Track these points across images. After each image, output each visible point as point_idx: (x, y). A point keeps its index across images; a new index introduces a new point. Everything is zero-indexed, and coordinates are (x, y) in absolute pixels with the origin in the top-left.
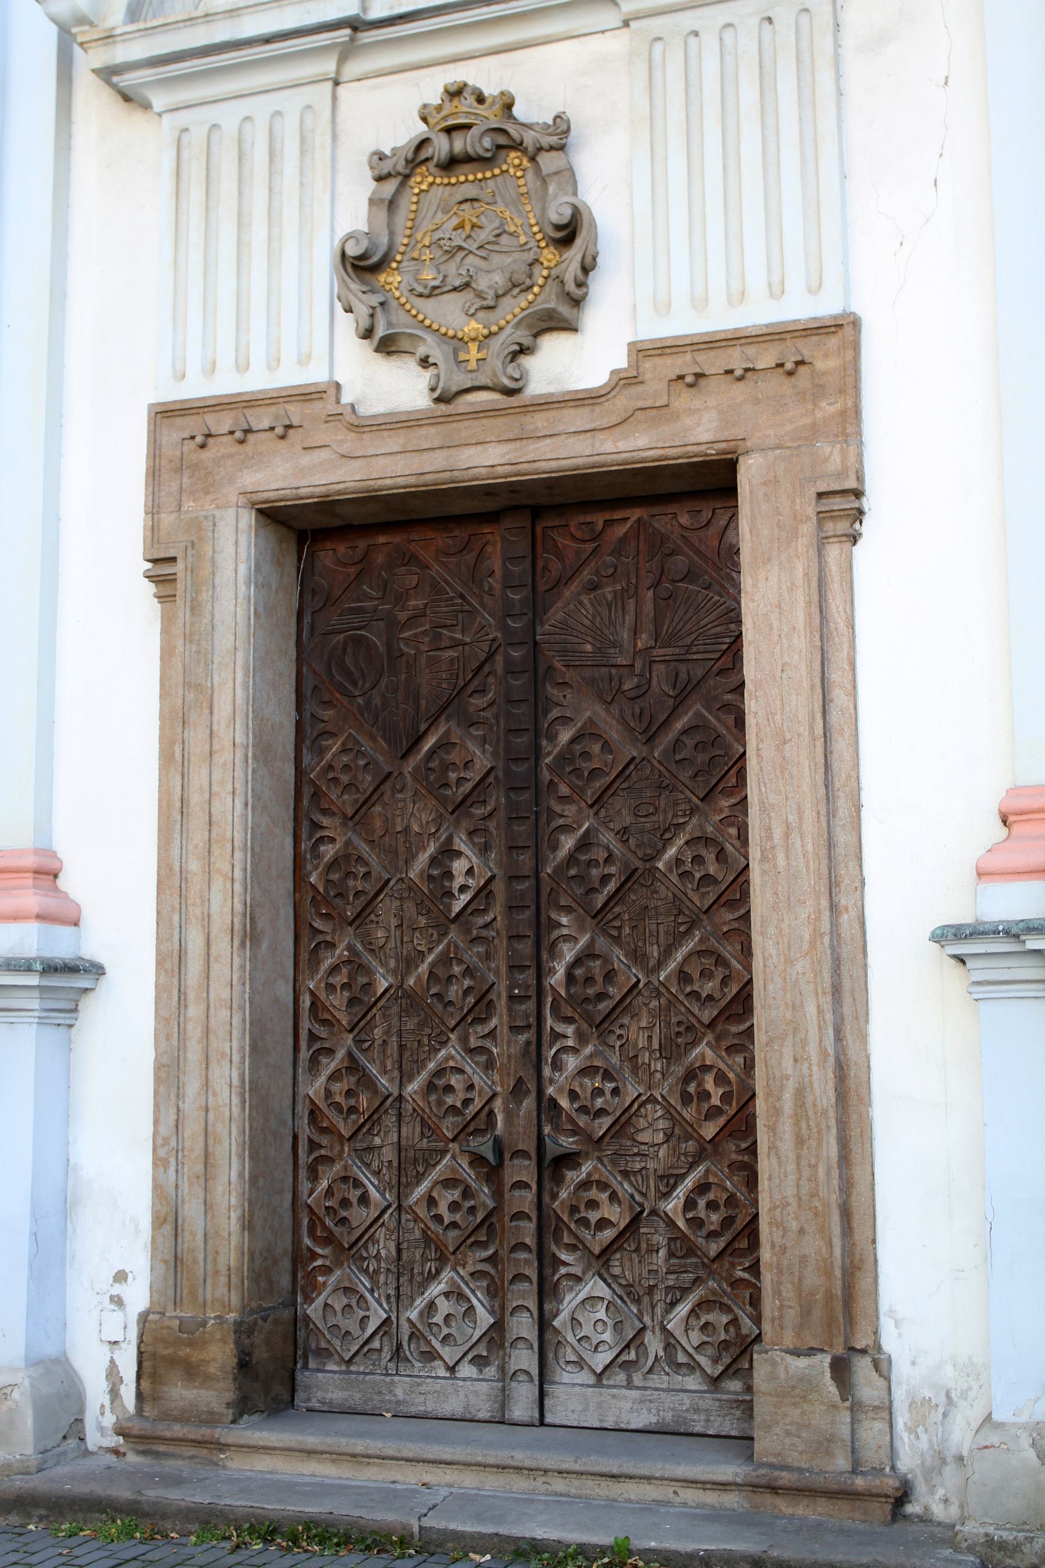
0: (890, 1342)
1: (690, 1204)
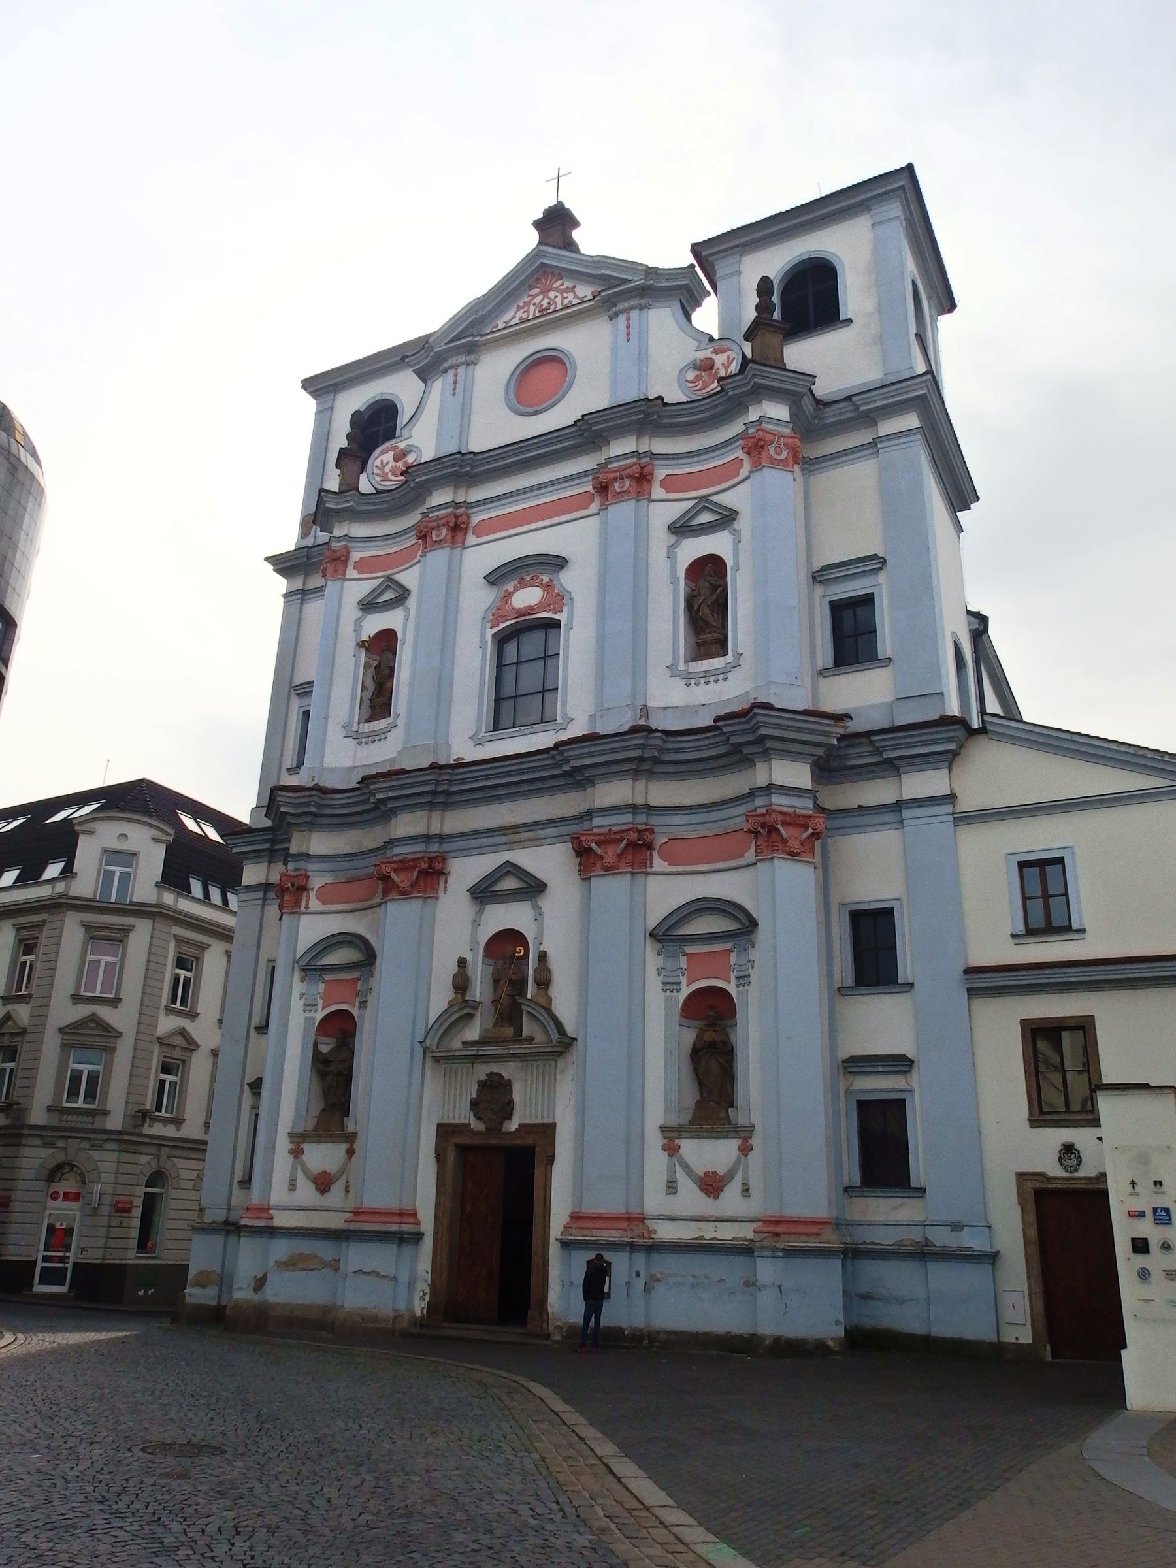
0: (549, 1310)
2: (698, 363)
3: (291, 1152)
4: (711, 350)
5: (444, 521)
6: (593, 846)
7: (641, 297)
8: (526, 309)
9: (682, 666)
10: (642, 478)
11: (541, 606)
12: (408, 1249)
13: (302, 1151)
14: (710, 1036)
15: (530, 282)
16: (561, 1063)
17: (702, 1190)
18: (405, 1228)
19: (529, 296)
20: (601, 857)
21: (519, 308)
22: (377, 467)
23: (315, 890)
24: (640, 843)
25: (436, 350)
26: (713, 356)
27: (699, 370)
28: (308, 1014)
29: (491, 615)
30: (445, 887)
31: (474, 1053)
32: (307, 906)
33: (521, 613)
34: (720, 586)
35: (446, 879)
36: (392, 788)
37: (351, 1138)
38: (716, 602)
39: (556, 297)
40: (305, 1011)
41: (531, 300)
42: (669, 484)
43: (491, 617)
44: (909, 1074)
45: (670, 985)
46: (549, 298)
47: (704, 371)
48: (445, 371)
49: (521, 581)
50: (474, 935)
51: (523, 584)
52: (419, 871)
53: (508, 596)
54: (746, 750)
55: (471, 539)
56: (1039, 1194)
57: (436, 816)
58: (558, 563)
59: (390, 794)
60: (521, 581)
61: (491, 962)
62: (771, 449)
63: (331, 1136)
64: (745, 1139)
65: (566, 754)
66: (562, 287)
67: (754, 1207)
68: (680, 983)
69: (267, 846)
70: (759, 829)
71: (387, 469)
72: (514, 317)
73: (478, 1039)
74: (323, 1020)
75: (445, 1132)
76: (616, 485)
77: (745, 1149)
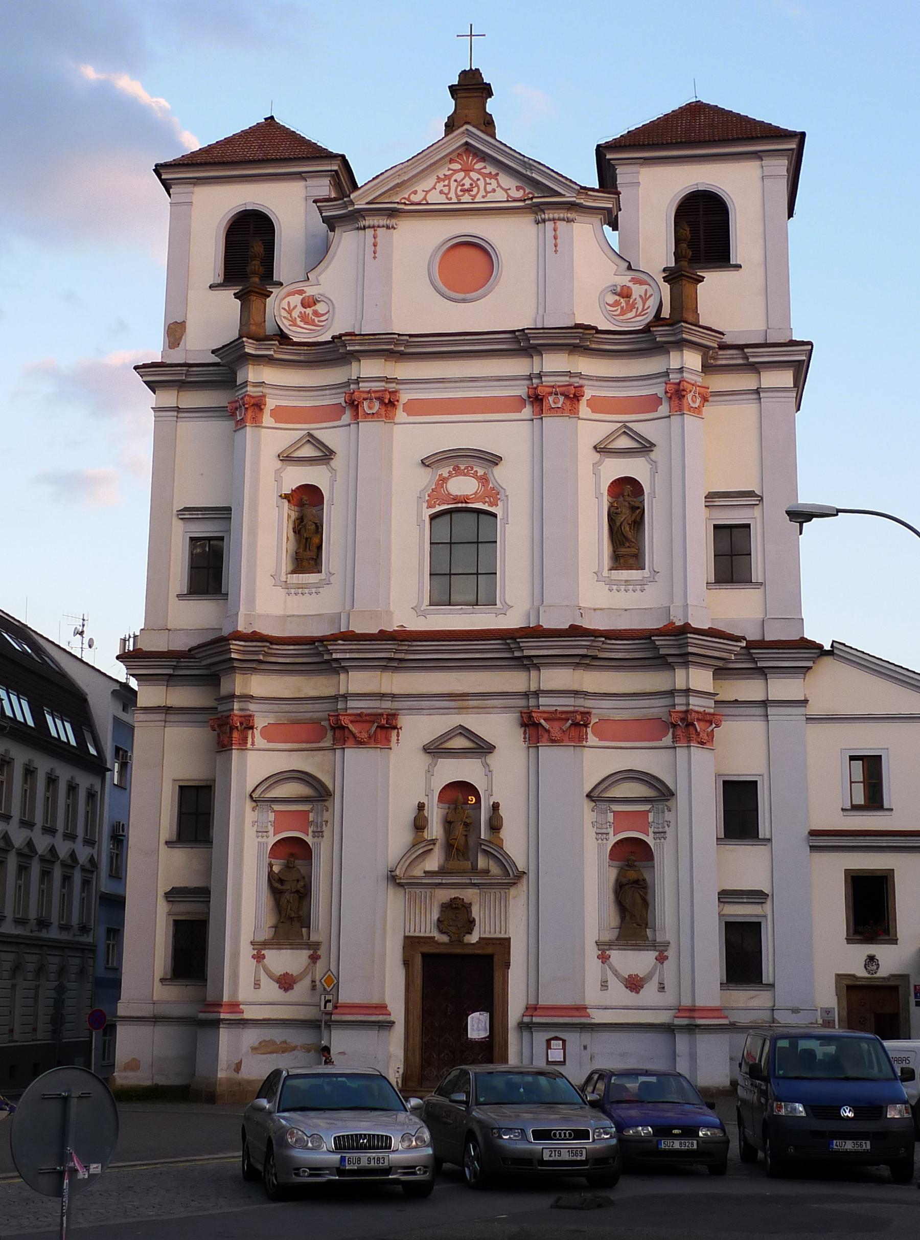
1: (481, 1058)
2: (619, 289)
3: (254, 957)
4: (629, 278)
5: (378, 395)
6: (542, 721)
7: (569, 209)
8: (446, 183)
9: (606, 573)
10: (573, 397)
11: (477, 498)
12: (384, 1033)
13: (264, 957)
14: (632, 875)
15: (451, 156)
16: (513, 891)
17: (627, 988)
18: (381, 1018)
19: (449, 169)
20: (548, 731)
21: (439, 179)
22: (284, 309)
23: (259, 729)
24: (582, 723)
25: (356, 207)
26: (630, 284)
27: (619, 295)
28: (260, 839)
29: (427, 495)
30: (398, 740)
31: (440, 881)
32: (253, 744)
33: (457, 500)
34: (638, 508)
35: (398, 733)
36: (351, 651)
37: (315, 946)
38: (635, 522)
39: (478, 179)
40: (258, 837)
41: (452, 175)
42: (597, 405)
43: (427, 498)
44: (763, 905)
45: (601, 835)
46: (471, 179)
47: (623, 298)
48: (364, 228)
49: (457, 468)
50: (428, 782)
51: (457, 471)
52: (377, 727)
53: (444, 480)
54: (670, 660)
55: (400, 415)
56: (849, 987)
57: (387, 675)
58: (494, 460)
59: (348, 656)
60: (457, 468)
61: (441, 805)
62: (689, 397)
63: (291, 944)
64: (661, 952)
65: (521, 645)
66: (484, 171)
67: (668, 999)
68: (608, 834)
69: (170, 671)
70: (679, 722)
71: (295, 314)
72: (434, 188)
73: (437, 869)
74: (275, 844)
75: (411, 943)
76: (551, 399)
77: (661, 959)
